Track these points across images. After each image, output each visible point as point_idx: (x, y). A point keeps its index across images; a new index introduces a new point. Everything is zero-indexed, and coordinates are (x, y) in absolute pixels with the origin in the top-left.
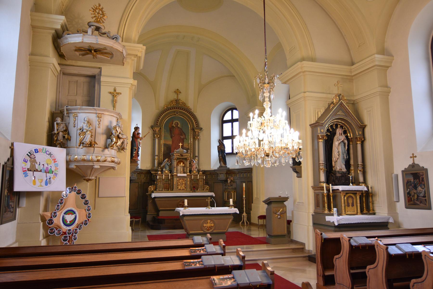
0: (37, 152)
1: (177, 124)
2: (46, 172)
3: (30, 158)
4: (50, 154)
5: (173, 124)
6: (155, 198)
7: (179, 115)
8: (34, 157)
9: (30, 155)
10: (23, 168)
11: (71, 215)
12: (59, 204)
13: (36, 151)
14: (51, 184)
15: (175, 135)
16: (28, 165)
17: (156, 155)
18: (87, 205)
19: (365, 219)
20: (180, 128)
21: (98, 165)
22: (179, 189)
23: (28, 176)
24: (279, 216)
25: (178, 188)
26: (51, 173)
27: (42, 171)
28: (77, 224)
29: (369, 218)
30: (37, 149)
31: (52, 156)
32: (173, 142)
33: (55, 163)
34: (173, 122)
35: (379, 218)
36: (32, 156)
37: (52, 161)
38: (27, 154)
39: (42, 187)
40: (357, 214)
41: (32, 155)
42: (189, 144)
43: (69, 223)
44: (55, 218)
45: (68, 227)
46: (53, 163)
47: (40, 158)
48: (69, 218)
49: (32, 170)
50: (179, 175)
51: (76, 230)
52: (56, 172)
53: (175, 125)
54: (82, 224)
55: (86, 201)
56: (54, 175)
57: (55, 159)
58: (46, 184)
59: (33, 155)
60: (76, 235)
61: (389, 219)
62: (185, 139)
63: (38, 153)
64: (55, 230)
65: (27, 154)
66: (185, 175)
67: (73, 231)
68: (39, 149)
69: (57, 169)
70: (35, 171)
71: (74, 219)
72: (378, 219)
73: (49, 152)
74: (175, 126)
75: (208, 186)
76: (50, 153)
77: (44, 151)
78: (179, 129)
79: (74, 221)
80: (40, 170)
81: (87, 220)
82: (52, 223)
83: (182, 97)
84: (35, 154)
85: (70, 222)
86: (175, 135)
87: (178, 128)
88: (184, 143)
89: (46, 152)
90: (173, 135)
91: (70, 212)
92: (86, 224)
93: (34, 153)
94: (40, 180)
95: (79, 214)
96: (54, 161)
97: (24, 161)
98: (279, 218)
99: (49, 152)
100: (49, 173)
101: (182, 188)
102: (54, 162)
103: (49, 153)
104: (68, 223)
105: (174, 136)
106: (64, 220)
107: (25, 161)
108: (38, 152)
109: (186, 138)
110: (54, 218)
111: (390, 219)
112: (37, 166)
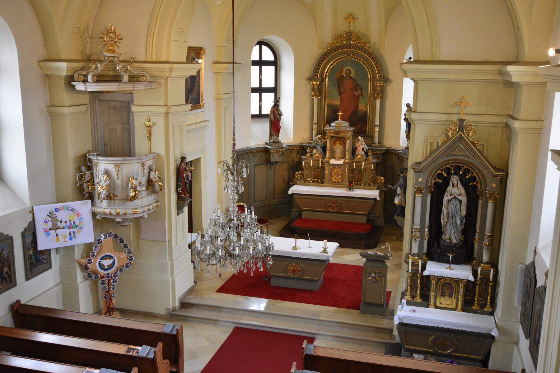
0: (57, 211)
1: (349, 73)
2: (69, 228)
3: (51, 217)
4: (73, 210)
6: (292, 194)
7: (352, 57)
8: (55, 216)
9: (51, 215)
10: (44, 229)
11: (108, 260)
12: (94, 251)
13: (57, 210)
14: (76, 238)
15: (345, 91)
16: (50, 225)
17: (314, 122)
18: (127, 249)
19: (447, 323)
20: (353, 78)
21: (120, 217)
22: (333, 182)
23: (50, 235)
24: (373, 279)
25: (331, 180)
26: (76, 227)
27: (65, 227)
28: (117, 267)
29: (453, 324)
30: (58, 208)
31: (75, 211)
32: (342, 101)
33: (79, 217)
34: (342, 69)
35: (473, 326)
36: (53, 216)
37: (76, 216)
38: (48, 215)
39: (67, 243)
40: (455, 310)
41: (52, 214)
42: (367, 104)
43: (107, 267)
44: (91, 264)
45: (106, 271)
46: (77, 217)
47: (62, 216)
48: (106, 263)
49: (54, 229)
50: (332, 161)
51: (115, 273)
52: (81, 226)
53: (346, 74)
54: (123, 267)
55: (125, 245)
56: (79, 229)
57: (79, 213)
58: (71, 239)
59: (53, 215)
60: (116, 278)
61: (491, 330)
62: (361, 96)
63: (59, 211)
64: (92, 275)
65: (48, 215)
66: (341, 162)
67: (112, 275)
68: (60, 207)
69: (81, 223)
70: (57, 229)
71: (113, 264)
72: (469, 328)
73: (71, 208)
74: (345, 76)
75: (382, 178)
76: (73, 208)
77: (65, 208)
78: (352, 81)
79: (112, 265)
80: (62, 227)
81: (129, 263)
82: (88, 269)
83: (358, 27)
84: (55, 213)
85: (108, 266)
86: (345, 91)
87: (350, 78)
88: (360, 102)
89: (68, 209)
91: (109, 257)
92: (127, 267)
93: (54, 212)
94: (64, 236)
95: (118, 258)
96: (77, 215)
97: (45, 222)
98: (374, 282)
99: (71, 208)
100: (72, 228)
101: (337, 181)
102: (78, 217)
103: (71, 209)
104: (106, 268)
106: (101, 266)
107: (46, 222)
108: (59, 210)
109: (362, 95)
110: (89, 264)
111: (493, 330)
112: (59, 224)
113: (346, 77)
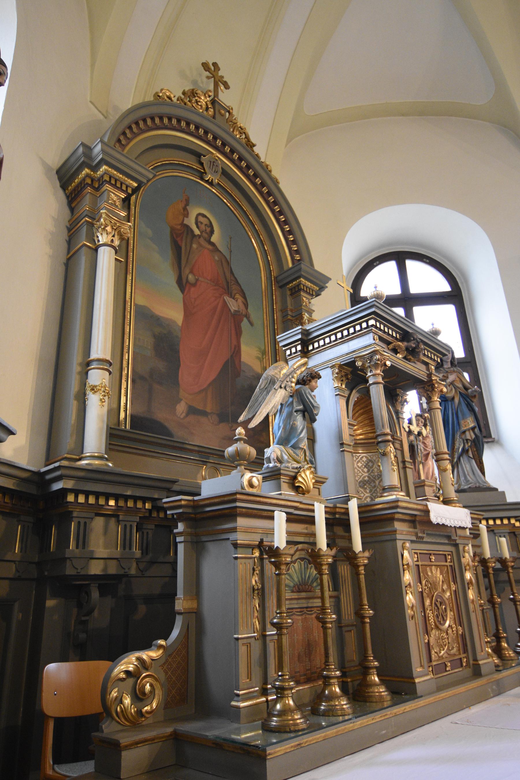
1: (208, 230)
5: (186, 215)
34: (187, 204)
62: (245, 320)
86: (197, 280)
87: (210, 247)
90: (191, 277)
105: (194, 285)
109: (247, 316)
113: (199, 236)
